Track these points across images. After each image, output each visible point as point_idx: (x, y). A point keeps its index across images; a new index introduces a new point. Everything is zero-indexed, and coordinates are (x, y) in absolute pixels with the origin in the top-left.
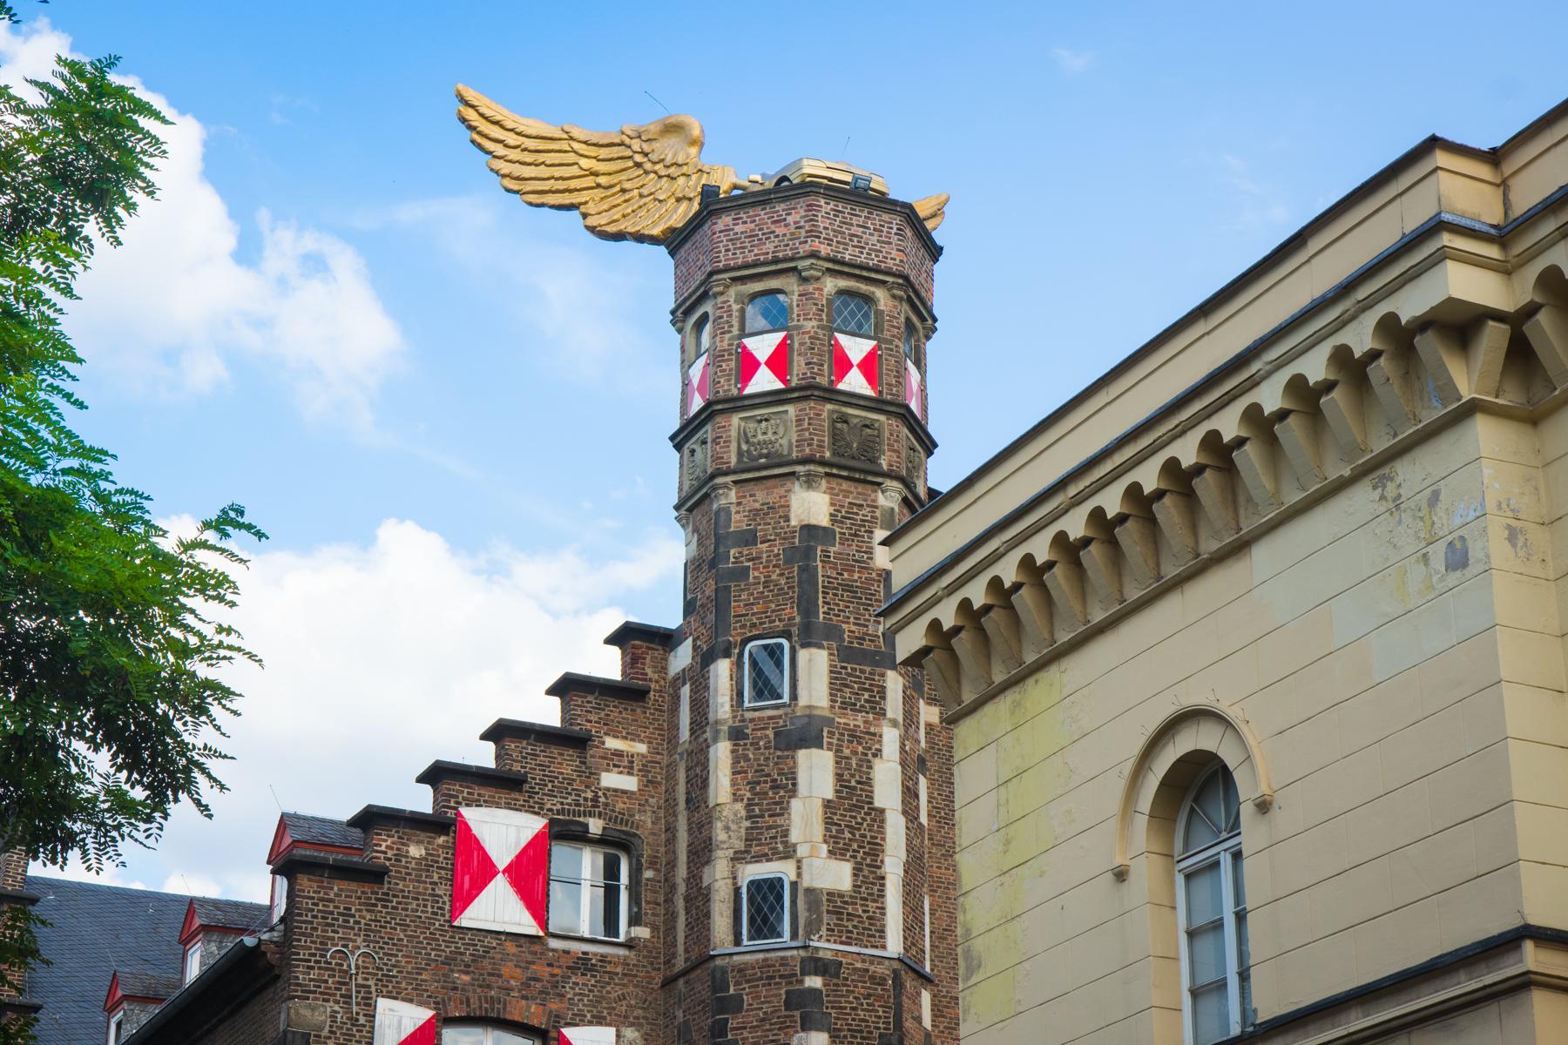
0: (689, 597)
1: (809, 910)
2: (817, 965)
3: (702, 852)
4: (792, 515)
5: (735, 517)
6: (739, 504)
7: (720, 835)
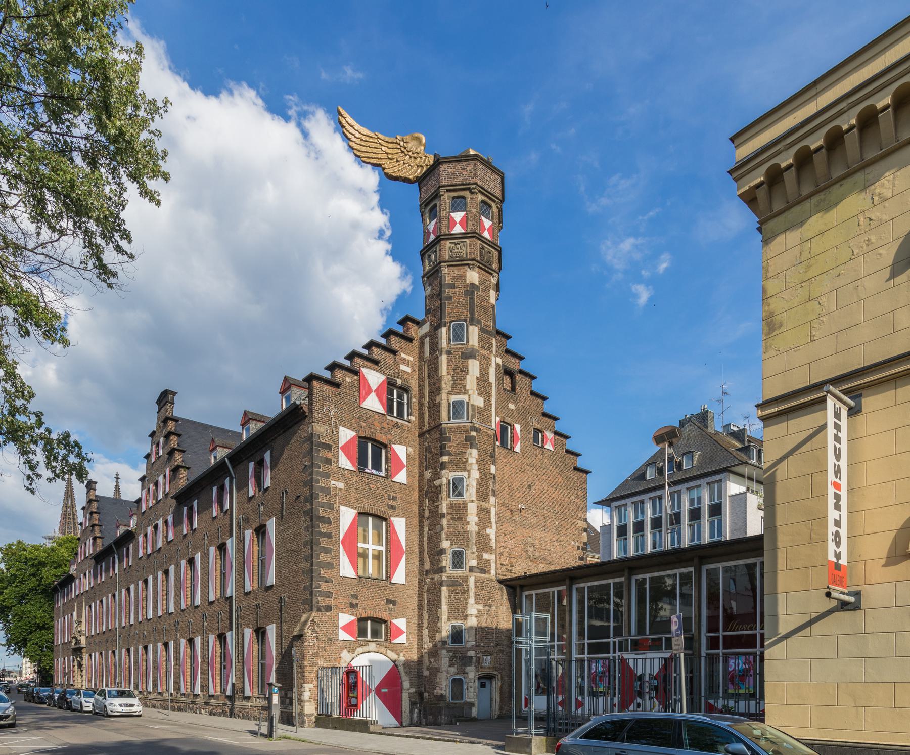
0: (427, 308)
1: (472, 411)
2: (477, 430)
4: (467, 279)
5: (447, 278)
6: (449, 274)
7: (444, 386)
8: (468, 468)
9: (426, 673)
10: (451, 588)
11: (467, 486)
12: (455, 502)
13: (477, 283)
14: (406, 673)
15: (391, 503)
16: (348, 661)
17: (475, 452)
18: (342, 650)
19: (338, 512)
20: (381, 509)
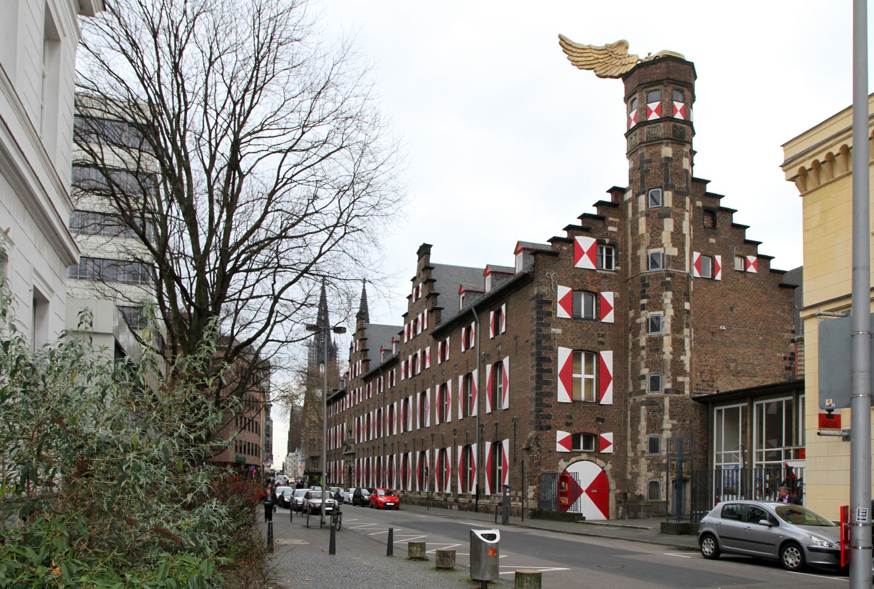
3: (636, 247)
8: (664, 307)
9: (629, 477)
11: (663, 322)
13: (670, 155)
14: (613, 477)
15: (601, 339)
16: (564, 468)
17: (670, 294)
18: (559, 459)
19: (557, 352)
20: (591, 346)
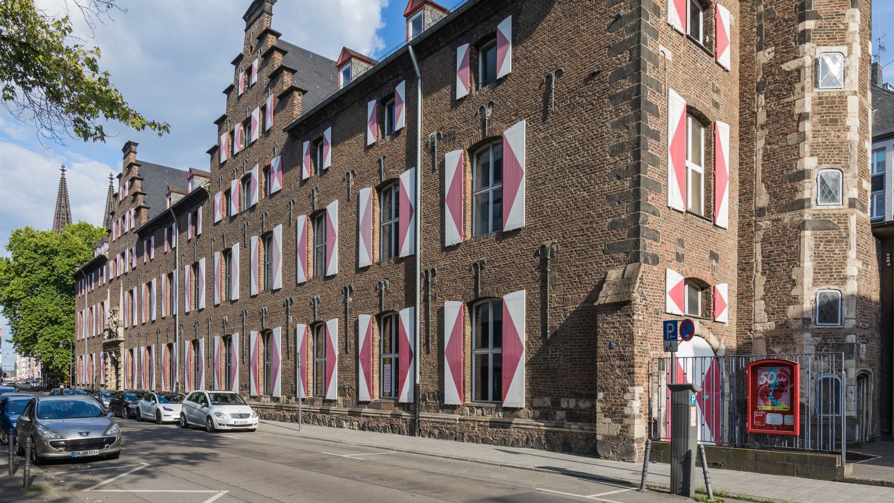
8: (848, 40)
10: (818, 232)
12: (827, 95)
